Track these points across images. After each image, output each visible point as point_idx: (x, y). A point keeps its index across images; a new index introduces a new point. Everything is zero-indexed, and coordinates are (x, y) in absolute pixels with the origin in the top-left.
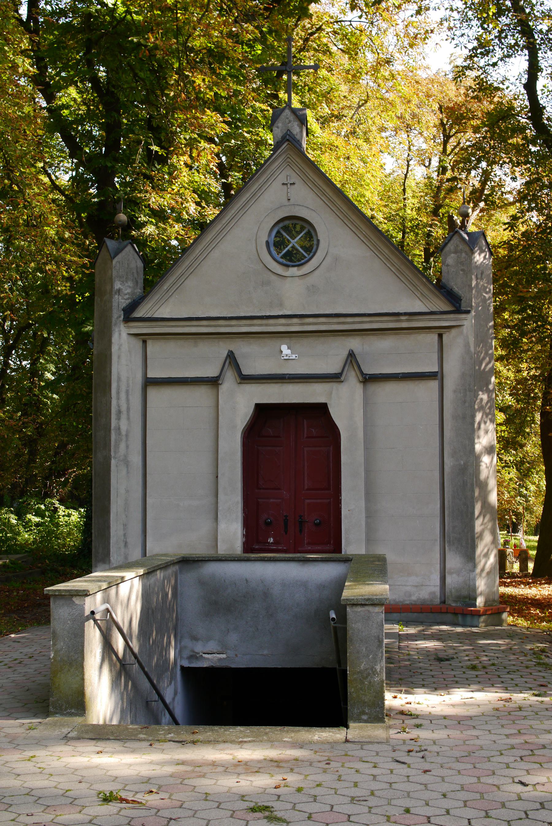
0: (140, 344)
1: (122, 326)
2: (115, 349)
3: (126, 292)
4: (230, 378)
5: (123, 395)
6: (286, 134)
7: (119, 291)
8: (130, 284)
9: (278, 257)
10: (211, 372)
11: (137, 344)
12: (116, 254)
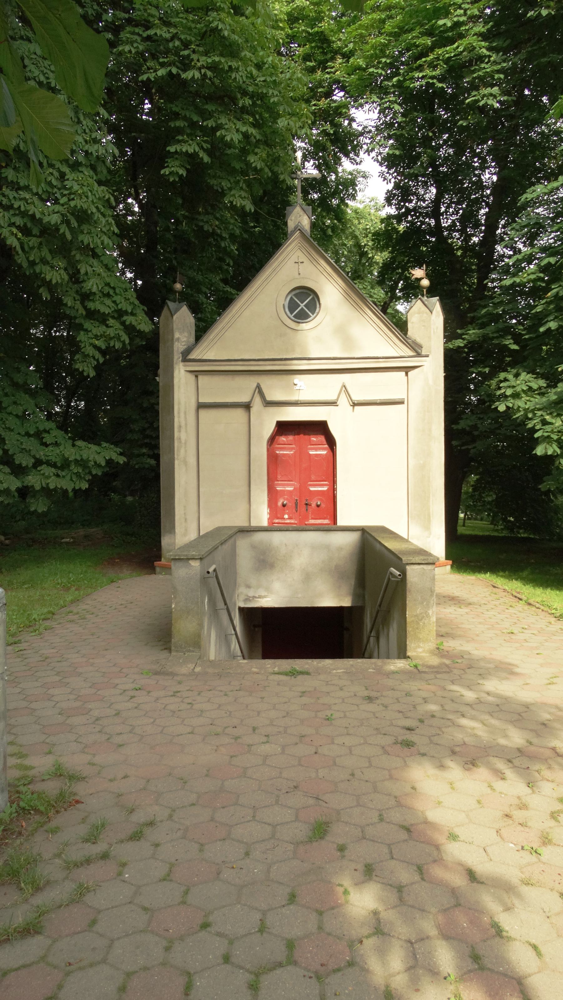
0: (194, 378)
1: (181, 364)
2: (176, 381)
3: (183, 340)
4: (257, 404)
5: (182, 415)
6: (298, 226)
7: (178, 339)
8: (186, 334)
9: (291, 316)
10: (244, 398)
11: (192, 378)
12: (175, 313)
